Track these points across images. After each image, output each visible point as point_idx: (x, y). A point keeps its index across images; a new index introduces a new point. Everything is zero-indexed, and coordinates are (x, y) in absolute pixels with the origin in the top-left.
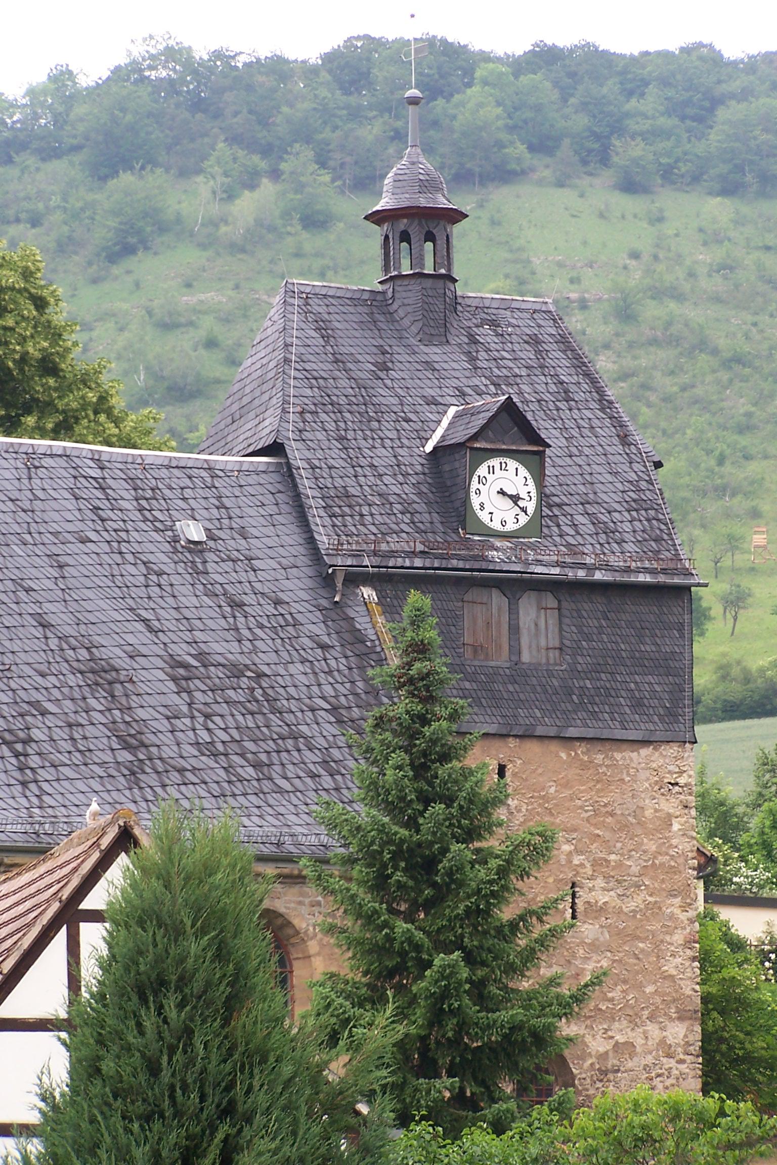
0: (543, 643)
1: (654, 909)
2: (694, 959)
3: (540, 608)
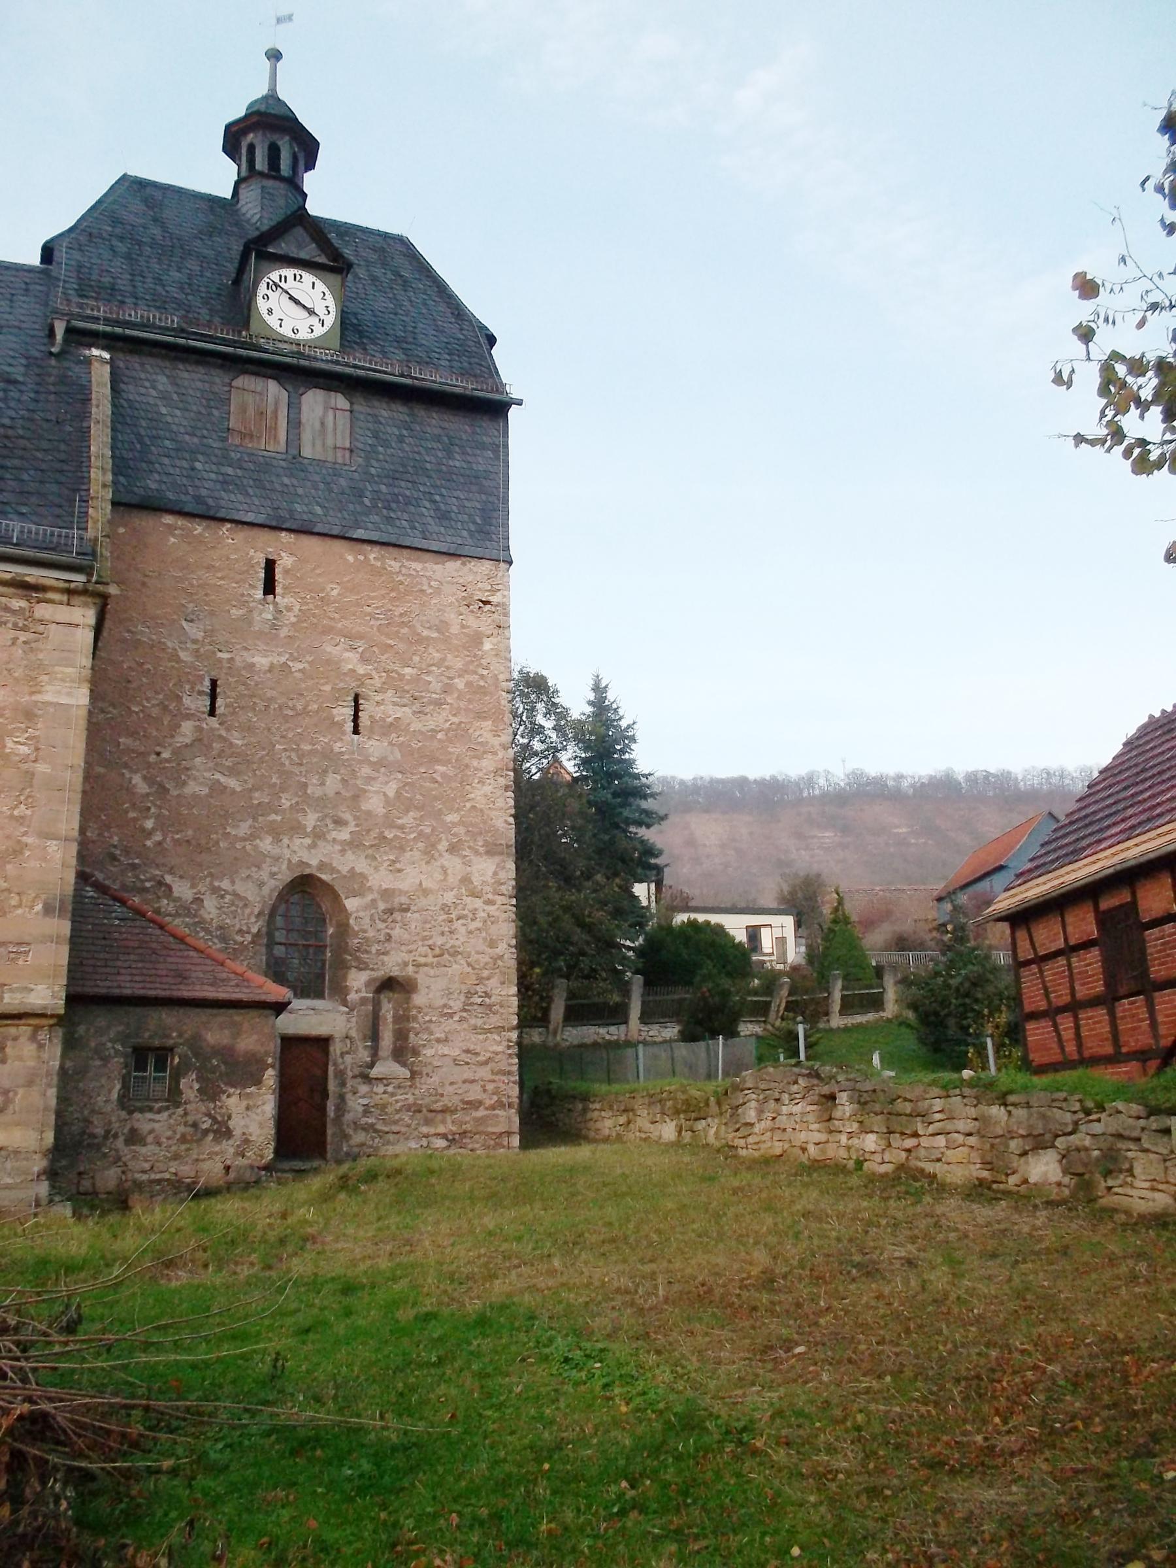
0: (330, 442)
1: (459, 733)
2: (507, 788)
3: (327, 408)
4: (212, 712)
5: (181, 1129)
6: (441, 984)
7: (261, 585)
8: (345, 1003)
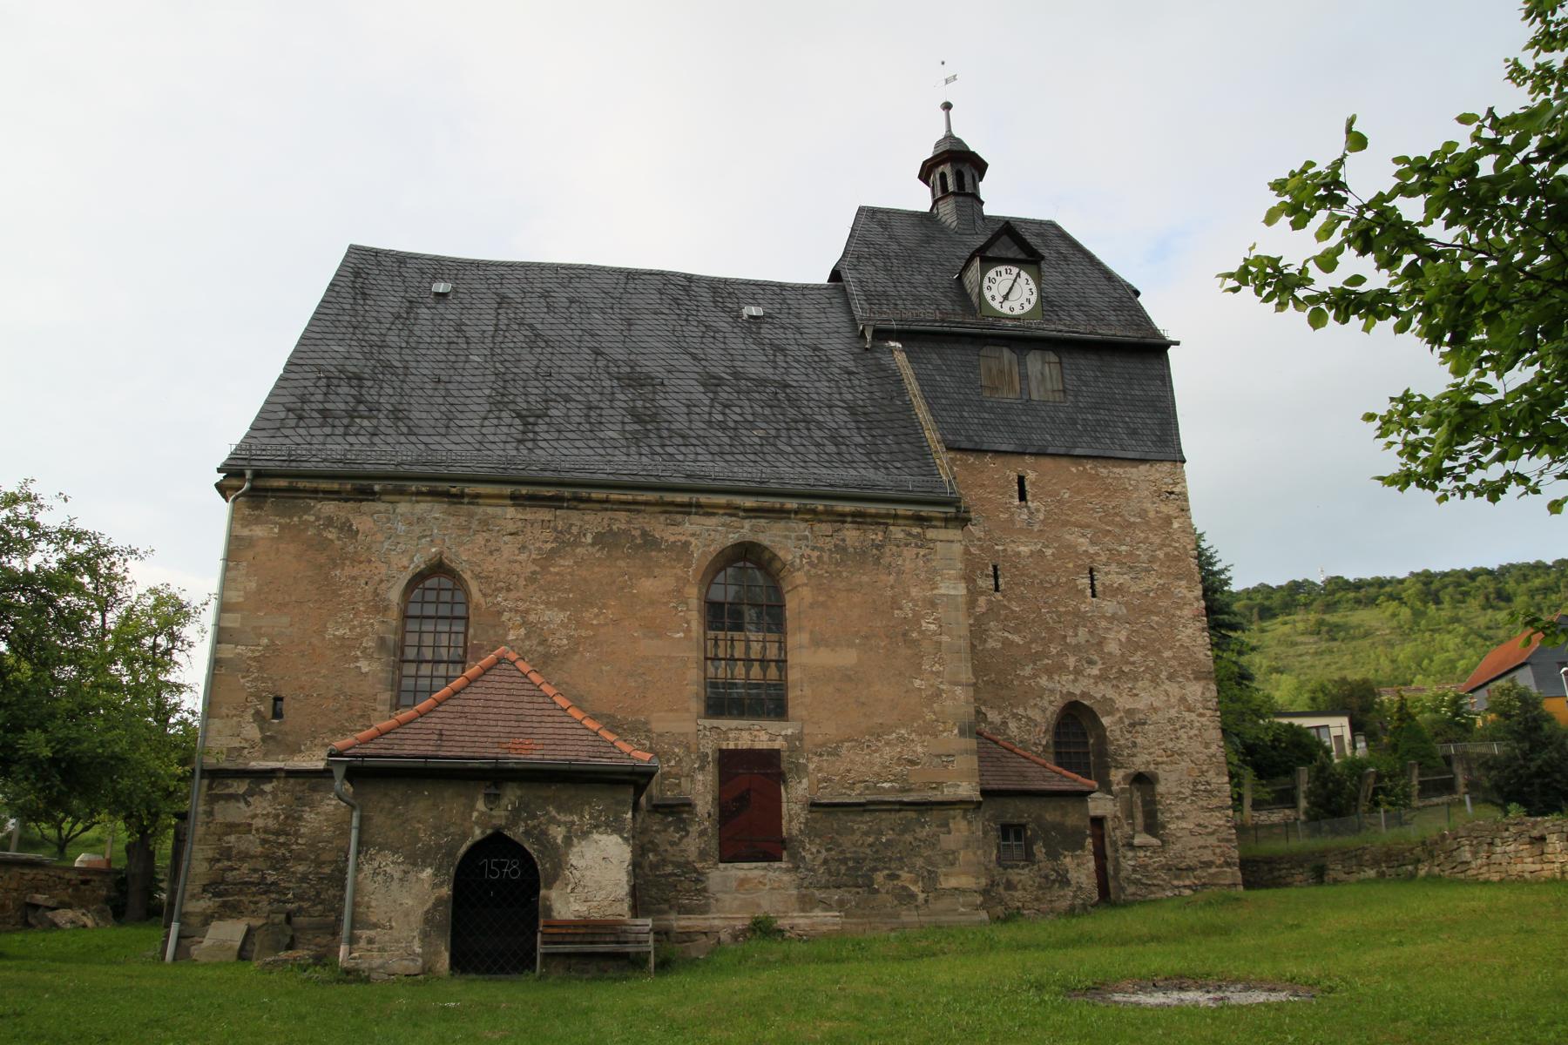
0: (1049, 386)
1: (1165, 591)
2: (1203, 630)
3: (1044, 362)
4: (997, 589)
5: (1038, 880)
6: (1174, 776)
7: (1016, 495)
8: (1110, 792)
